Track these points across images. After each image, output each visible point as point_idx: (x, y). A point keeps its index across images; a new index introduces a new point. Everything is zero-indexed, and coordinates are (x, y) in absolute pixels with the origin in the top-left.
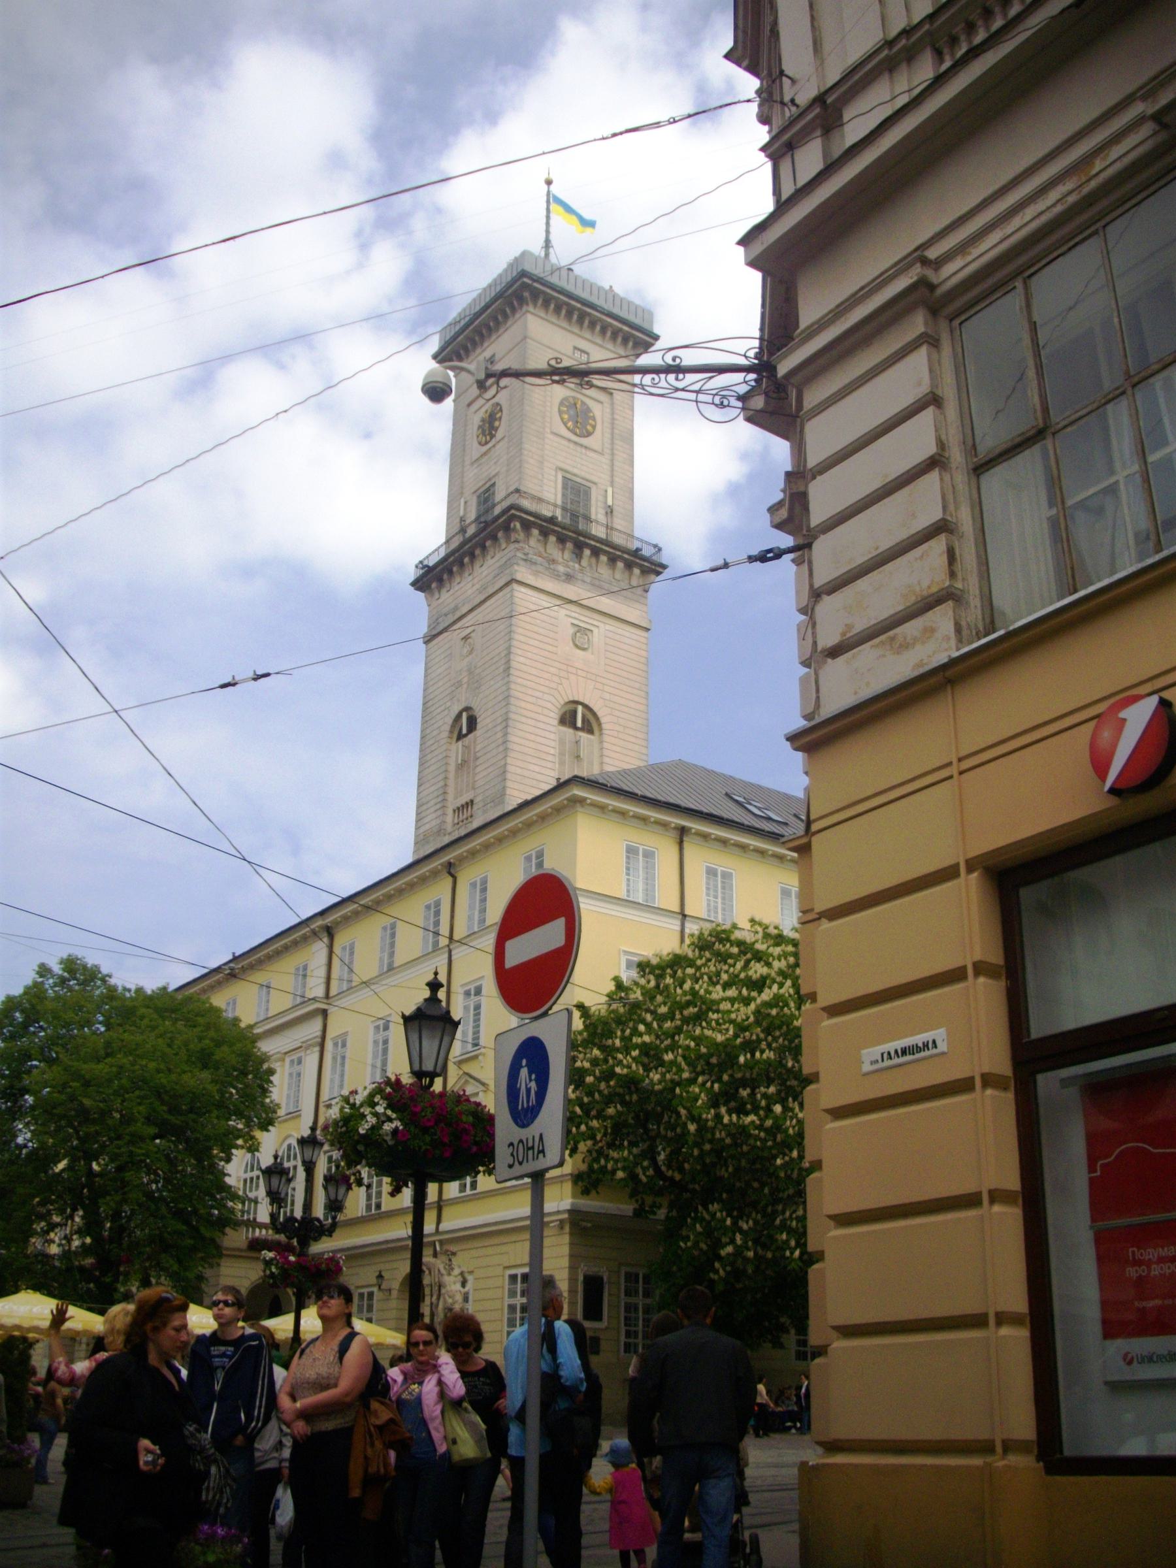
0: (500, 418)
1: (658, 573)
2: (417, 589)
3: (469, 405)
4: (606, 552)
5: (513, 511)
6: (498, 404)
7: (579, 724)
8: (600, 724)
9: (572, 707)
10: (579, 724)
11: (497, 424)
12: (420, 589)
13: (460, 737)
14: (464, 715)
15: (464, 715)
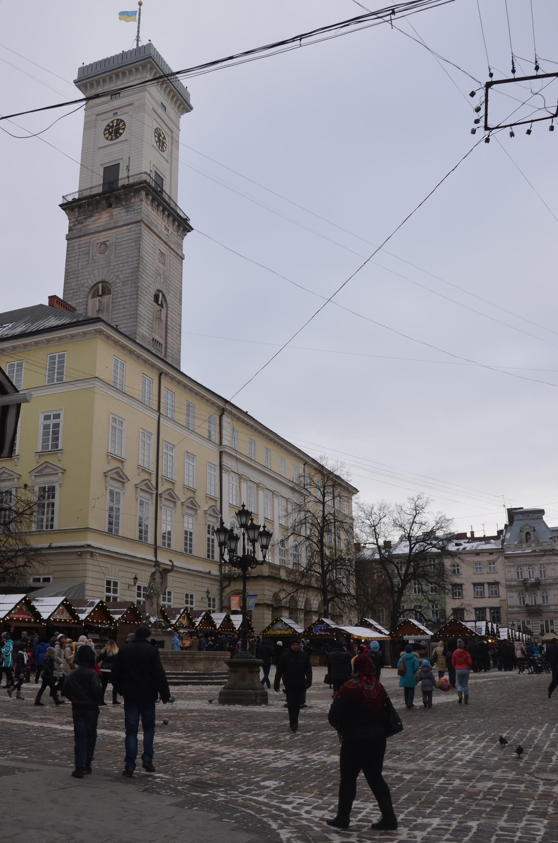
0: (124, 129)
1: (189, 231)
2: (63, 209)
3: (97, 115)
4: (173, 216)
5: (145, 184)
6: (122, 121)
7: (160, 303)
8: (167, 304)
9: (157, 293)
10: (160, 303)
11: (121, 131)
12: (64, 209)
13: (96, 295)
14: (100, 285)
15: (100, 285)
